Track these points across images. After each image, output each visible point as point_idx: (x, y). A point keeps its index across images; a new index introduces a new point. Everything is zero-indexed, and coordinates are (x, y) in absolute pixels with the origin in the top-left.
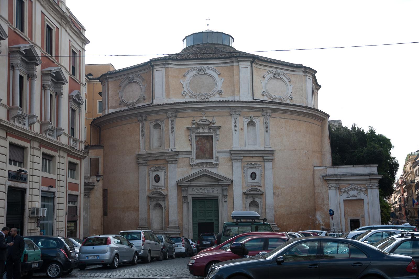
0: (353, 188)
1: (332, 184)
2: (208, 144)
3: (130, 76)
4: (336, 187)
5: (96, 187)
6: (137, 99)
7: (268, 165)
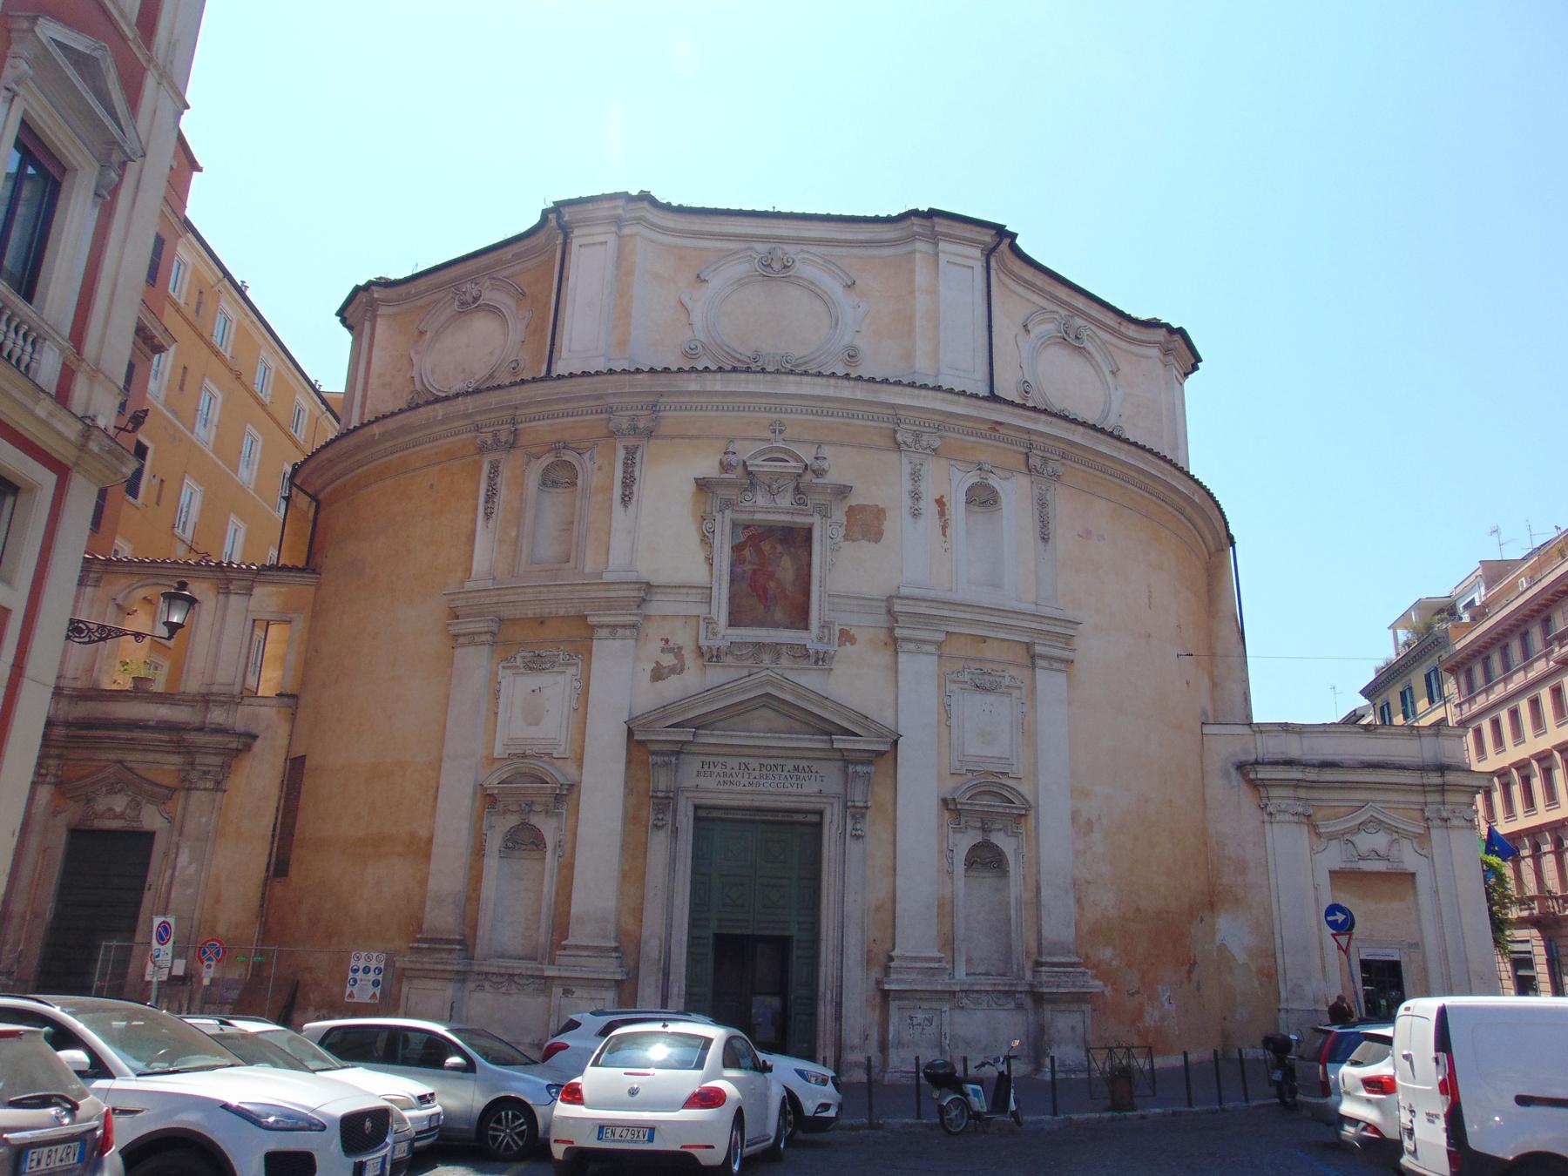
0: (1373, 820)
7: (1049, 682)
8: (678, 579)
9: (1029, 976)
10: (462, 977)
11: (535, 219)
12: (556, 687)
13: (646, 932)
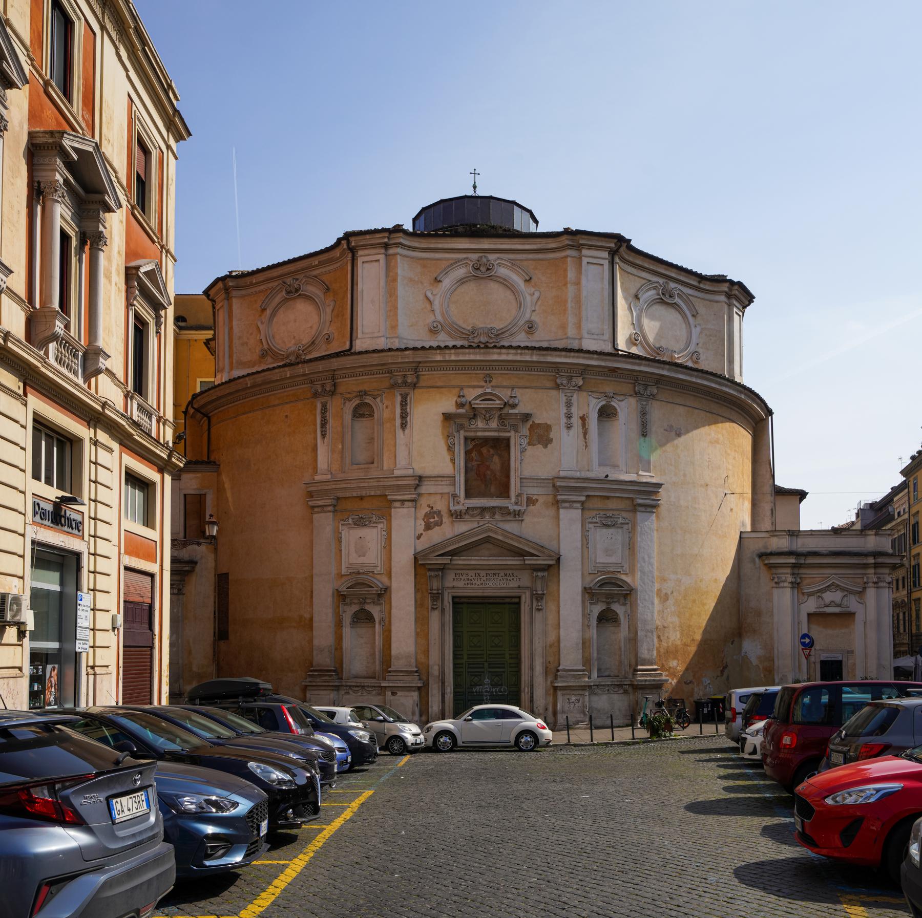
2: (496, 459)
8: (435, 472)
9: (631, 676)
10: (337, 688)
11: (332, 242)
12: (372, 535)
13: (431, 663)
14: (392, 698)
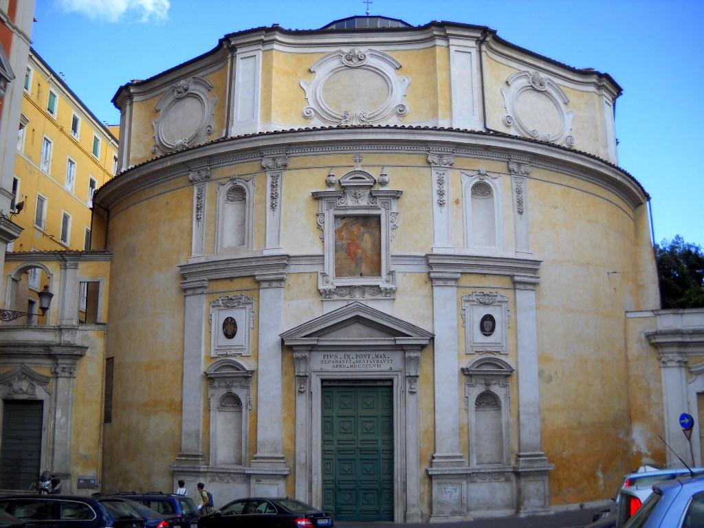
1: (673, 355)
2: (367, 237)
3: (182, 82)
4: (679, 362)
5: (88, 353)
6: (192, 133)
7: (525, 298)
9: (513, 462)
11: (215, 44)
14: (256, 486)
